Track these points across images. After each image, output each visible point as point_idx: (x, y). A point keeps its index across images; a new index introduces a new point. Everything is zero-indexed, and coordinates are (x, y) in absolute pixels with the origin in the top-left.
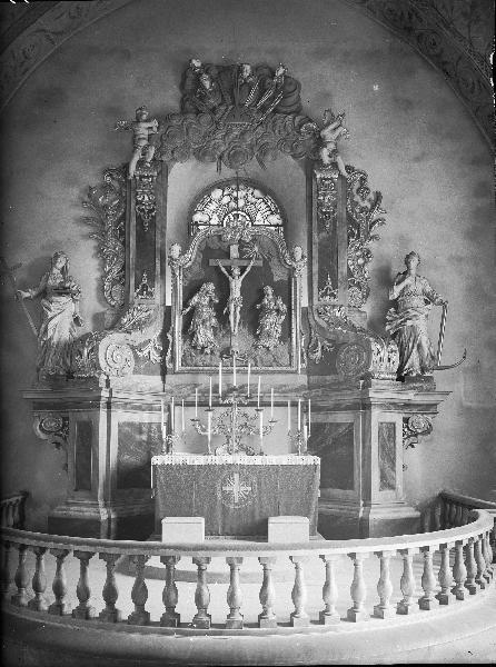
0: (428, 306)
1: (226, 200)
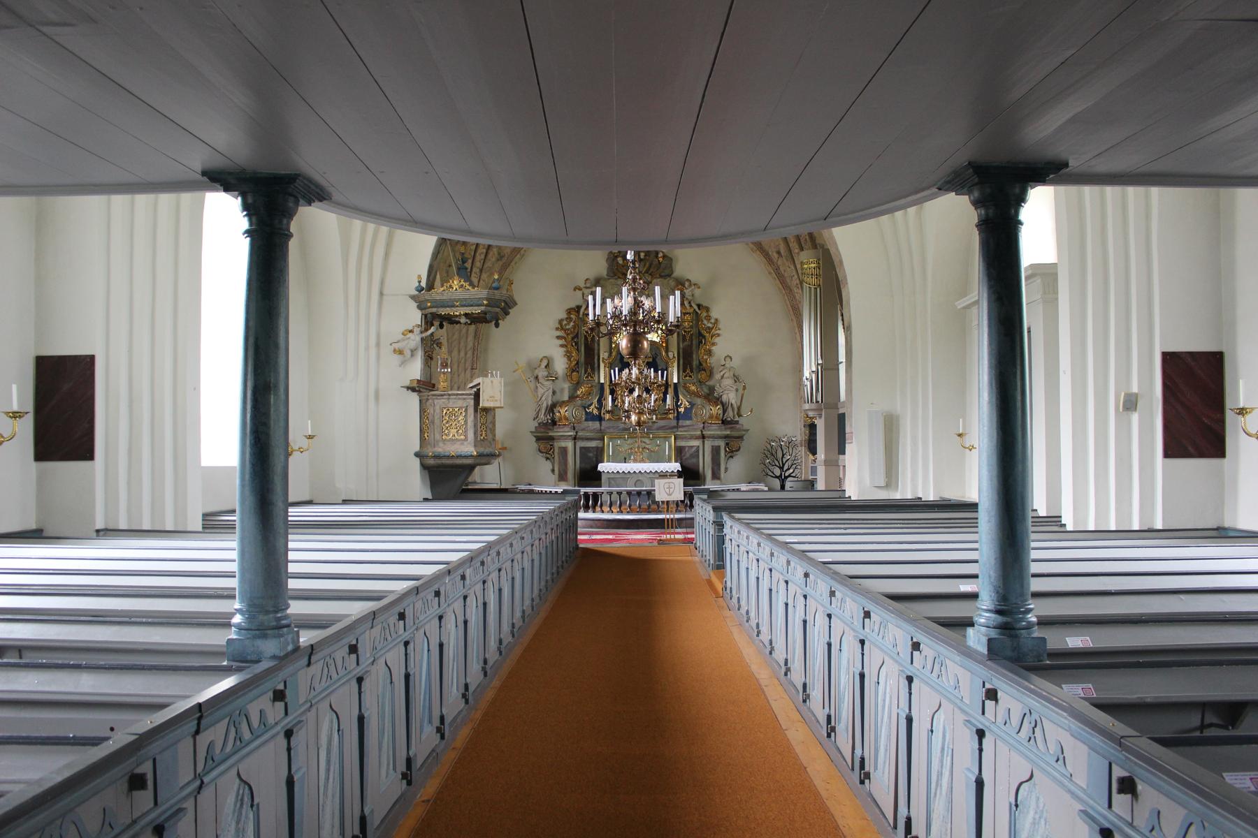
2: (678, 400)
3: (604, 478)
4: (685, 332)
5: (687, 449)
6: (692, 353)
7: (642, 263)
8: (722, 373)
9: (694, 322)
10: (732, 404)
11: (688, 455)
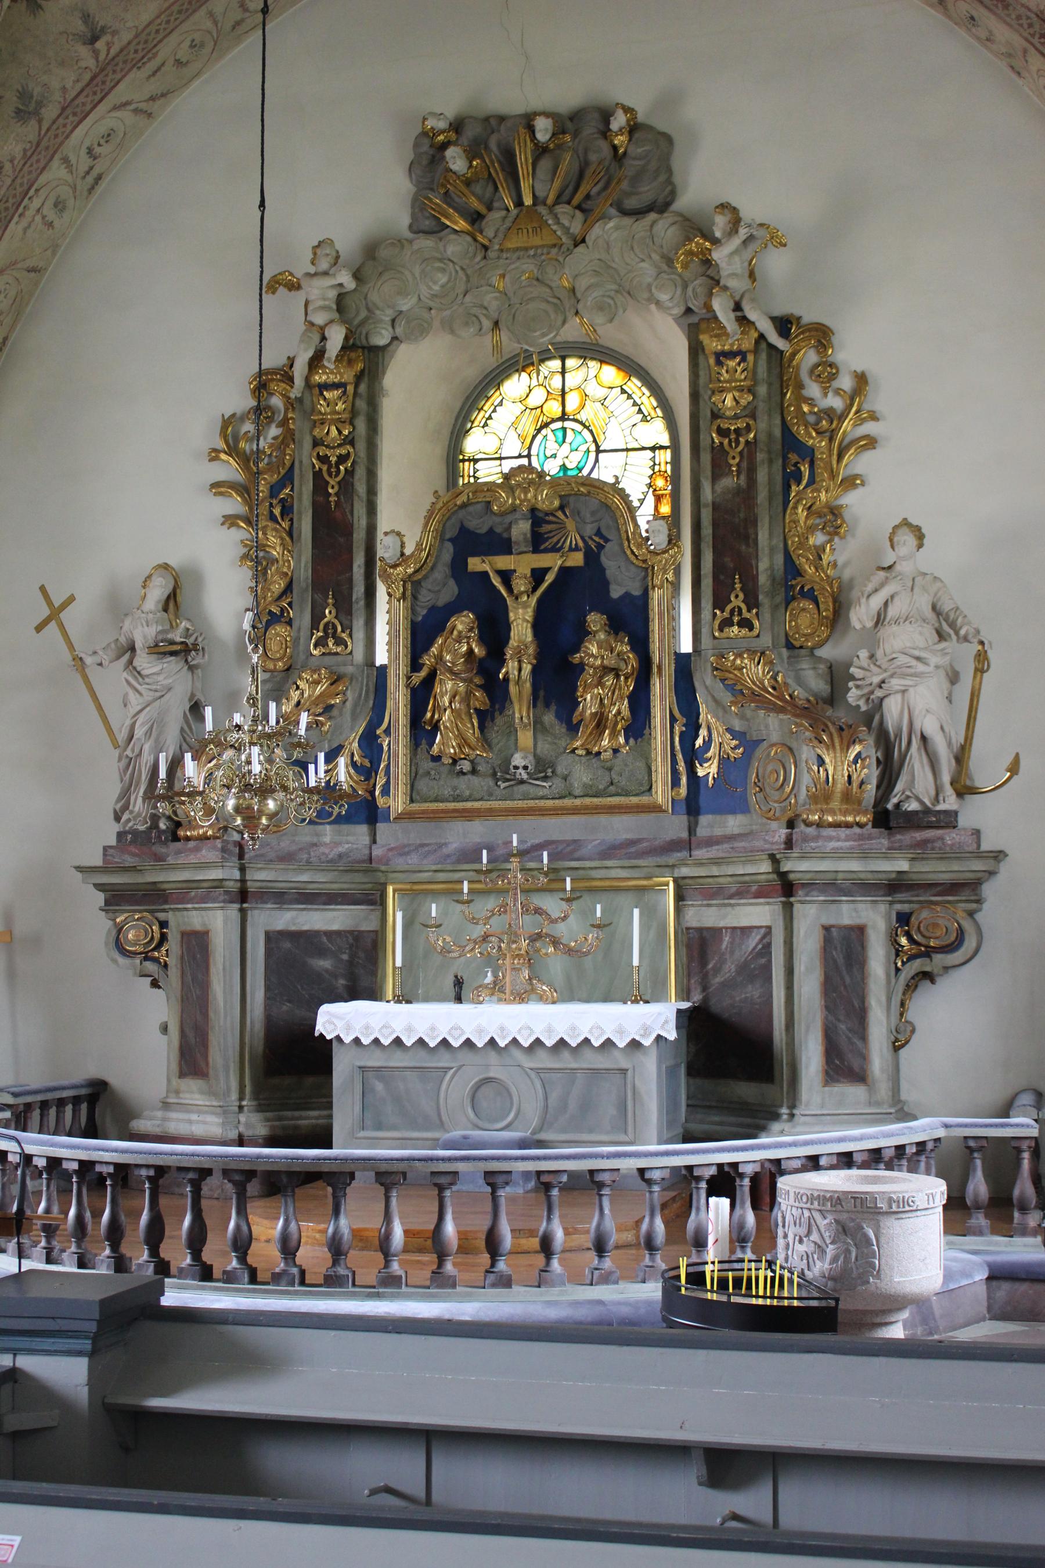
0: (943, 645)
1: (538, 397)
2: (693, 727)
3: (342, 1066)
4: (723, 433)
5: (727, 939)
6: (752, 522)
7: (545, 164)
8: (876, 602)
9: (762, 390)
10: (924, 738)
11: (730, 968)
